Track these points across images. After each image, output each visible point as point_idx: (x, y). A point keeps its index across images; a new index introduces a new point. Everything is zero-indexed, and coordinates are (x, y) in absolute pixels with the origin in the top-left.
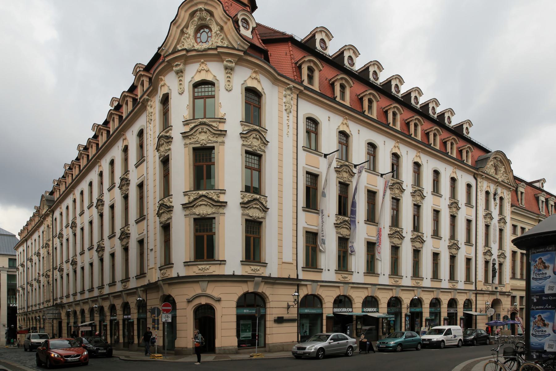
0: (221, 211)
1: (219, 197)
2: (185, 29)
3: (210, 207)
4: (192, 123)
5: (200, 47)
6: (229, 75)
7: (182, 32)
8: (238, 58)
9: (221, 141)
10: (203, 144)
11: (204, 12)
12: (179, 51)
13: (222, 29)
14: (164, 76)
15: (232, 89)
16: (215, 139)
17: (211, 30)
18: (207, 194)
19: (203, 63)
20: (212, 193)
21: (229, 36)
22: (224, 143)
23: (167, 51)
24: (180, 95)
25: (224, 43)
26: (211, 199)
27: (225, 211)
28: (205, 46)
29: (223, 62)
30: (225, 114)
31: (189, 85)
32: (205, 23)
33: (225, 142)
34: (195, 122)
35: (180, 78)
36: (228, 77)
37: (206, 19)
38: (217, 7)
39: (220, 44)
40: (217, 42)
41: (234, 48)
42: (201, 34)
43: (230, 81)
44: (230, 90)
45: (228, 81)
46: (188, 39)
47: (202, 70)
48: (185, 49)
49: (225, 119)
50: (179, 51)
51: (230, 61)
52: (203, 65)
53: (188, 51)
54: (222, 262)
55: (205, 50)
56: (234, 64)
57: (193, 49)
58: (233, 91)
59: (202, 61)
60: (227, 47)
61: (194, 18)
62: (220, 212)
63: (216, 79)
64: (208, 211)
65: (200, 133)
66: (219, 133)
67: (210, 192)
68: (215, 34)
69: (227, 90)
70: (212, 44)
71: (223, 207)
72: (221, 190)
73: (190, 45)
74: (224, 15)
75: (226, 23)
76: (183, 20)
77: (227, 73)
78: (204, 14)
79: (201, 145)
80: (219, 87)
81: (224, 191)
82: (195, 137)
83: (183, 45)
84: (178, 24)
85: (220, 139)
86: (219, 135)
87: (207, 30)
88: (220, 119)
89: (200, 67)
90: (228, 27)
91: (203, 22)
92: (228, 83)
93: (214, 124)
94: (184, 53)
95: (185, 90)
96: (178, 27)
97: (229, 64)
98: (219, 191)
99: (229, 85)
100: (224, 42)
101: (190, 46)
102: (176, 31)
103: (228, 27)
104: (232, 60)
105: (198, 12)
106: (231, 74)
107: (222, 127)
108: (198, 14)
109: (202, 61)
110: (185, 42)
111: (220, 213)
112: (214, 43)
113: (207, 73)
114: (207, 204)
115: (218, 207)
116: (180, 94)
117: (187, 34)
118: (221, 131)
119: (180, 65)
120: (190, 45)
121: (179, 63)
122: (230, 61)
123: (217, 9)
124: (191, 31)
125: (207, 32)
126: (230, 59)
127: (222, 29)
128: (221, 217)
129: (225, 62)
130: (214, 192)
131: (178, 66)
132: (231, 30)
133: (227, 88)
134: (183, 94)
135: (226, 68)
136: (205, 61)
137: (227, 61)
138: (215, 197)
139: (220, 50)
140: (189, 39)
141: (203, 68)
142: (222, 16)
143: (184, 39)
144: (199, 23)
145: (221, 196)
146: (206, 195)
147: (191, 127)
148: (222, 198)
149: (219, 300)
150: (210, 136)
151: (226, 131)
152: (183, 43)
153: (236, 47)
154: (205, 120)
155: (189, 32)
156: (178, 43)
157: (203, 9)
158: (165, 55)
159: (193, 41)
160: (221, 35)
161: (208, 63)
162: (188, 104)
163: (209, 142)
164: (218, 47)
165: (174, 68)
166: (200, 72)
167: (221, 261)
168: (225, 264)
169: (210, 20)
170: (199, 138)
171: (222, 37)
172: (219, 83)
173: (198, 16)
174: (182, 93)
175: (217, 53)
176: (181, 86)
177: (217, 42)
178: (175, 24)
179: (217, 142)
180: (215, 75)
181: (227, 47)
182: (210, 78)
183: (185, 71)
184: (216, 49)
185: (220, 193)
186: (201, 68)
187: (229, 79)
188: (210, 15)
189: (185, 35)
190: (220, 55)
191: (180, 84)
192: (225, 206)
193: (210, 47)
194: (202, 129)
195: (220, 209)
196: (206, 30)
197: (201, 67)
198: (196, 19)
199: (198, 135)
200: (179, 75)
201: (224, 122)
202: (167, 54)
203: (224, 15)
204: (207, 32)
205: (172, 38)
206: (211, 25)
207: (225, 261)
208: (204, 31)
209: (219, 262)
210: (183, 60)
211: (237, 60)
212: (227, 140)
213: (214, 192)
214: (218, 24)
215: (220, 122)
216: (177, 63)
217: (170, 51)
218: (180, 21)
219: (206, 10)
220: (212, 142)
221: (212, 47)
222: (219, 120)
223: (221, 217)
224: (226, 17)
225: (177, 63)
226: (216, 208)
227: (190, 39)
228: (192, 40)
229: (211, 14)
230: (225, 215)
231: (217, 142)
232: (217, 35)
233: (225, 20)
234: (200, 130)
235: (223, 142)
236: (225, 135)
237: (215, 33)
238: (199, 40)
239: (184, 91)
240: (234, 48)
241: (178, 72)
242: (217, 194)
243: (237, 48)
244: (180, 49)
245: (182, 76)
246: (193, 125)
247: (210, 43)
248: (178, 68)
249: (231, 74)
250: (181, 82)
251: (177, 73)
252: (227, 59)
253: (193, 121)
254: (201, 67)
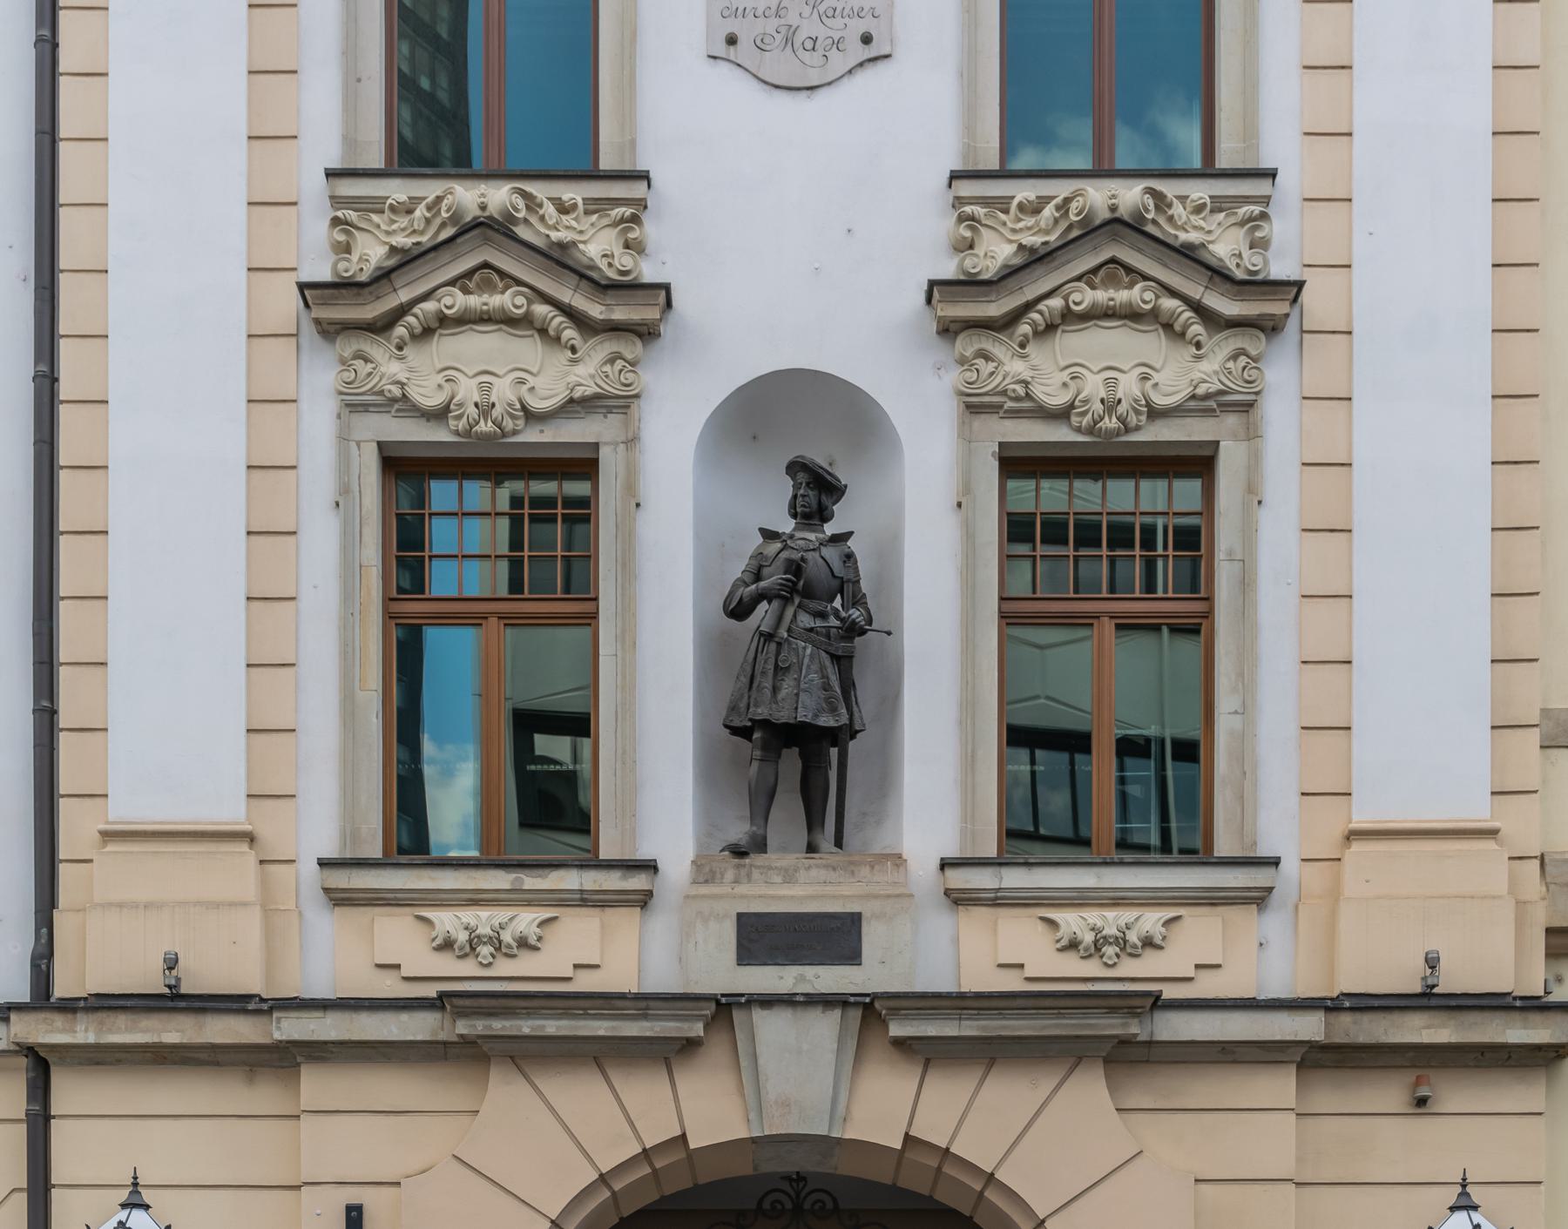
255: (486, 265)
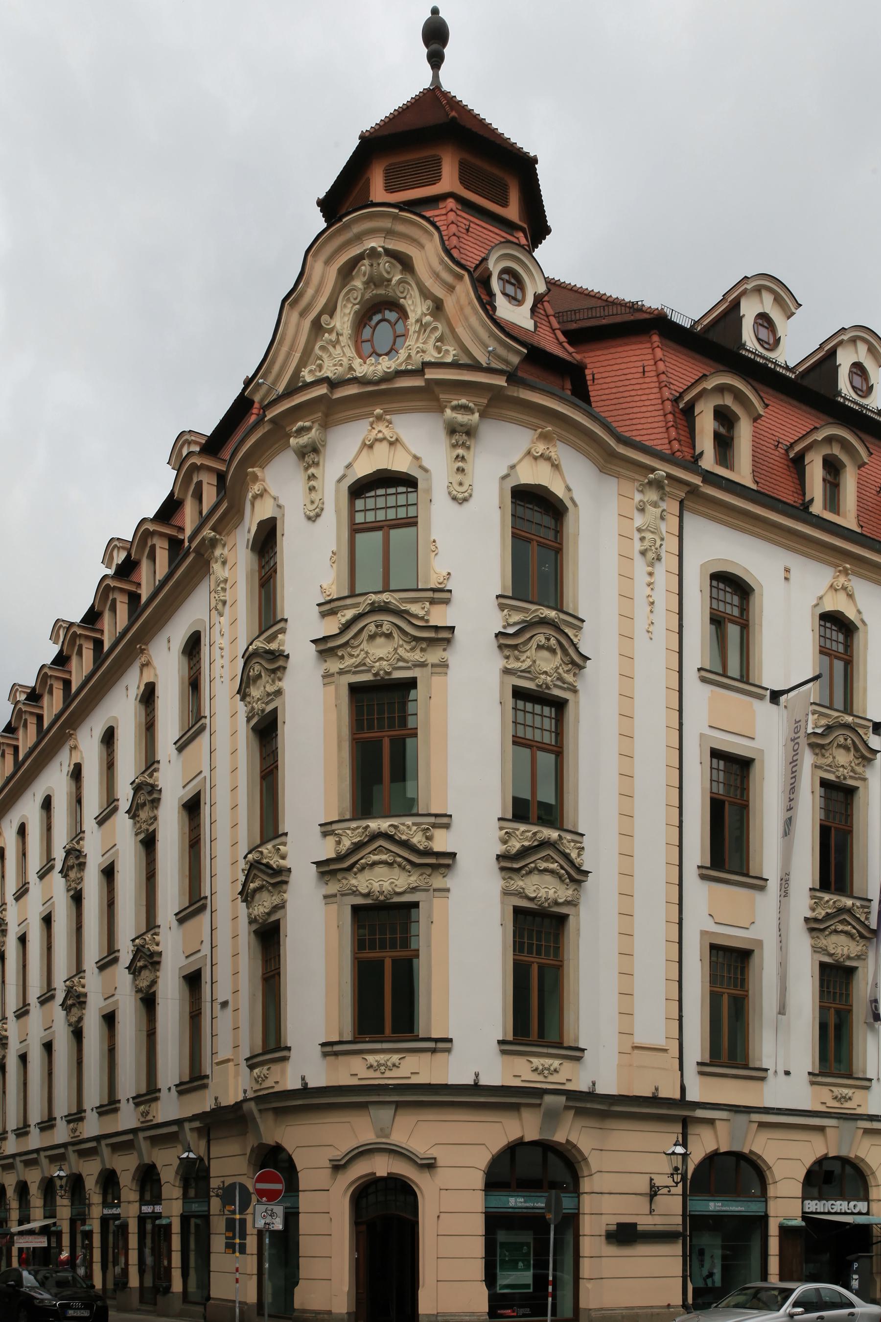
234: (372, 628)
255: (381, 846)
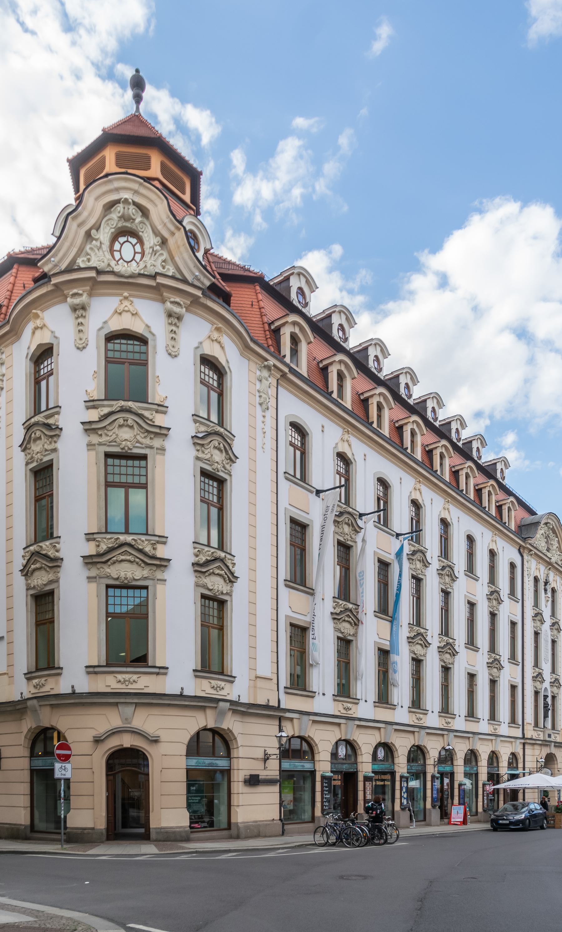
0: (159, 575)
1: (154, 549)
2: (93, 232)
3: (140, 565)
4: (103, 406)
5: (124, 269)
6: (174, 328)
7: (88, 235)
8: (191, 299)
9: (159, 447)
10: (126, 448)
11: (132, 207)
12: (80, 269)
13: (164, 242)
14: (42, 310)
15: (179, 354)
16: (147, 441)
17: (141, 241)
18: (133, 542)
19: (126, 298)
20: (143, 541)
21: (177, 259)
22: (164, 450)
23: (56, 266)
24: (78, 351)
25: (168, 269)
26: (141, 551)
27: (166, 575)
28: (134, 268)
29: (163, 301)
30: (166, 397)
31: (98, 336)
32: (131, 228)
33: (167, 448)
34: (111, 406)
35: (80, 320)
36: (172, 331)
37: (134, 220)
38: (157, 201)
39: (159, 269)
40: (154, 266)
41: (185, 281)
42: (122, 245)
43: (175, 339)
44: (176, 356)
45: (172, 338)
46: (98, 250)
47: (124, 311)
48: (95, 268)
49: (167, 407)
50: (80, 269)
51: (178, 304)
52: (126, 303)
53: (99, 272)
54: (162, 671)
55: (132, 276)
56: (184, 309)
57: (108, 269)
58: (179, 357)
59: (126, 294)
60: (173, 277)
61: (111, 213)
62: (159, 577)
63: (150, 332)
64: (135, 573)
65: (120, 426)
66: (157, 430)
67: (140, 539)
68: (151, 250)
69: (170, 354)
70: (146, 266)
71: (163, 568)
72: (159, 536)
73: (103, 262)
74: (171, 220)
75: (173, 234)
76: (90, 215)
77: (171, 324)
78: (132, 209)
79: (123, 449)
80: (155, 347)
81: (164, 540)
82: (110, 433)
83: (89, 260)
84: (80, 219)
85: (157, 443)
86: (156, 434)
87: (134, 241)
88: (159, 405)
89: (120, 305)
90: (176, 242)
91: (128, 224)
92: (173, 343)
93: (146, 414)
94: (93, 274)
95: (89, 343)
96: (80, 225)
97: (177, 309)
98: (157, 539)
99: (173, 347)
100: (167, 267)
101: (102, 263)
102: (76, 232)
103: (176, 242)
104: (182, 303)
105: (121, 205)
106: (178, 327)
107: (159, 420)
108: (120, 207)
109: (126, 294)
110: (92, 254)
111: (158, 580)
112: (148, 266)
113: (134, 317)
114: (134, 561)
115: (154, 568)
116: (78, 348)
117: (96, 240)
118: (160, 427)
119: (81, 295)
120: (103, 262)
121: (80, 292)
122: (178, 304)
123: (156, 206)
124: (104, 235)
125: (134, 243)
126: (178, 300)
127: (164, 242)
128: (159, 587)
129: (168, 305)
130: (146, 540)
131: (77, 297)
132: (182, 249)
133: (170, 351)
134: (84, 350)
135: (170, 315)
136: (131, 296)
137: (172, 302)
138: (148, 549)
139: (160, 280)
140: (100, 251)
141: (126, 309)
142: (166, 221)
143: (91, 249)
144: (120, 225)
145: (159, 546)
146: (133, 543)
147: (102, 413)
148: (162, 552)
149: (155, 741)
150: (139, 434)
151: (169, 429)
152: (88, 257)
153: (190, 278)
154: (130, 404)
155: (102, 239)
156: (78, 255)
157: (130, 200)
158: (52, 273)
159: (108, 256)
160: (162, 254)
161: (135, 300)
162: (96, 369)
163: (138, 445)
164: (157, 274)
165: (69, 299)
166: (120, 314)
167: (160, 668)
168: (165, 674)
169: (141, 222)
170: (117, 435)
171: (163, 258)
172: (155, 340)
173: (119, 212)
174: (84, 348)
175: (154, 284)
176: (81, 335)
177: (154, 266)
178: (74, 218)
179: (151, 447)
180: (149, 325)
181: (173, 277)
182: (138, 328)
183: (89, 307)
184: (153, 277)
185: (158, 542)
186: (122, 308)
187: (174, 335)
188: (140, 214)
189: (94, 242)
190: (159, 290)
191: (79, 331)
192: (166, 566)
193: (142, 272)
194: (124, 420)
195: (156, 572)
196: (130, 239)
197: (123, 306)
198: (114, 215)
199: (116, 430)
200: (79, 312)
201: (165, 413)
202: (56, 270)
203: (171, 220)
204: (134, 243)
205: (67, 244)
206: (143, 232)
207: (167, 668)
208: (127, 241)
209: (157, 670)
210: (88, 288)
211: (189, 303)
212: (168, 444)
213: (146, 540)
214: (156, 233)
215: (157, 411)
216: (75, 291)
217: (63, 266)
218: (85, 214)
219: (135, 203)
220: (143, 446)
221: (146, 273)
222: (156, 407)
223: (160, 587)
224: (174, 224)
225: (75, 291)
226: (150, 570)
227: (103, 252)
228: (106, 253)
229: (145, 212)
230: (167, 583)
231: (151, 447)
232: (154, 252)
233: (172, 228)
235: (162, 450)
236: (166, 435)
237: (150, 247)
238: (117, 255)
239: (87, 345)
240: (185, 281)
241: (77, 307)
242: (152, 544)
243: (191, 282)
244: (82, 266)
245: (85, 317)
246: (106, 410)
247: (142, 265)
248: (77, 301)
249: (178, 327)
250: (80, 328)
251: (74, 309)
252: (172, 300)
253: (106, 403)
254: (123, 306)
